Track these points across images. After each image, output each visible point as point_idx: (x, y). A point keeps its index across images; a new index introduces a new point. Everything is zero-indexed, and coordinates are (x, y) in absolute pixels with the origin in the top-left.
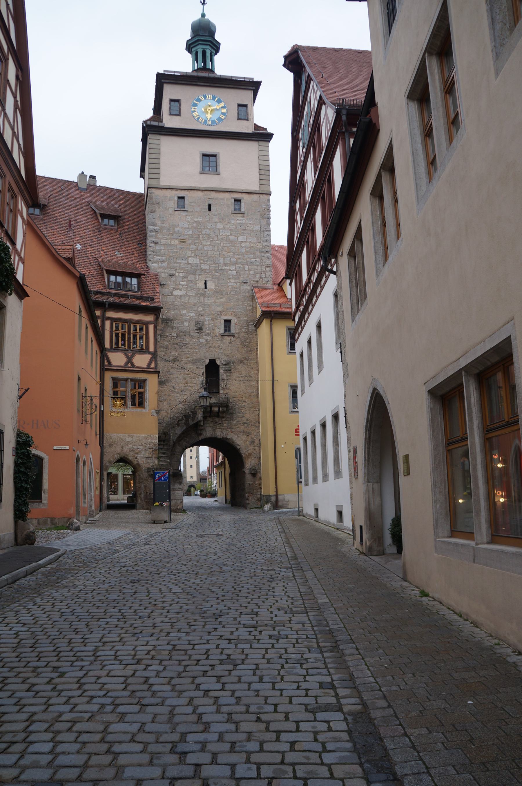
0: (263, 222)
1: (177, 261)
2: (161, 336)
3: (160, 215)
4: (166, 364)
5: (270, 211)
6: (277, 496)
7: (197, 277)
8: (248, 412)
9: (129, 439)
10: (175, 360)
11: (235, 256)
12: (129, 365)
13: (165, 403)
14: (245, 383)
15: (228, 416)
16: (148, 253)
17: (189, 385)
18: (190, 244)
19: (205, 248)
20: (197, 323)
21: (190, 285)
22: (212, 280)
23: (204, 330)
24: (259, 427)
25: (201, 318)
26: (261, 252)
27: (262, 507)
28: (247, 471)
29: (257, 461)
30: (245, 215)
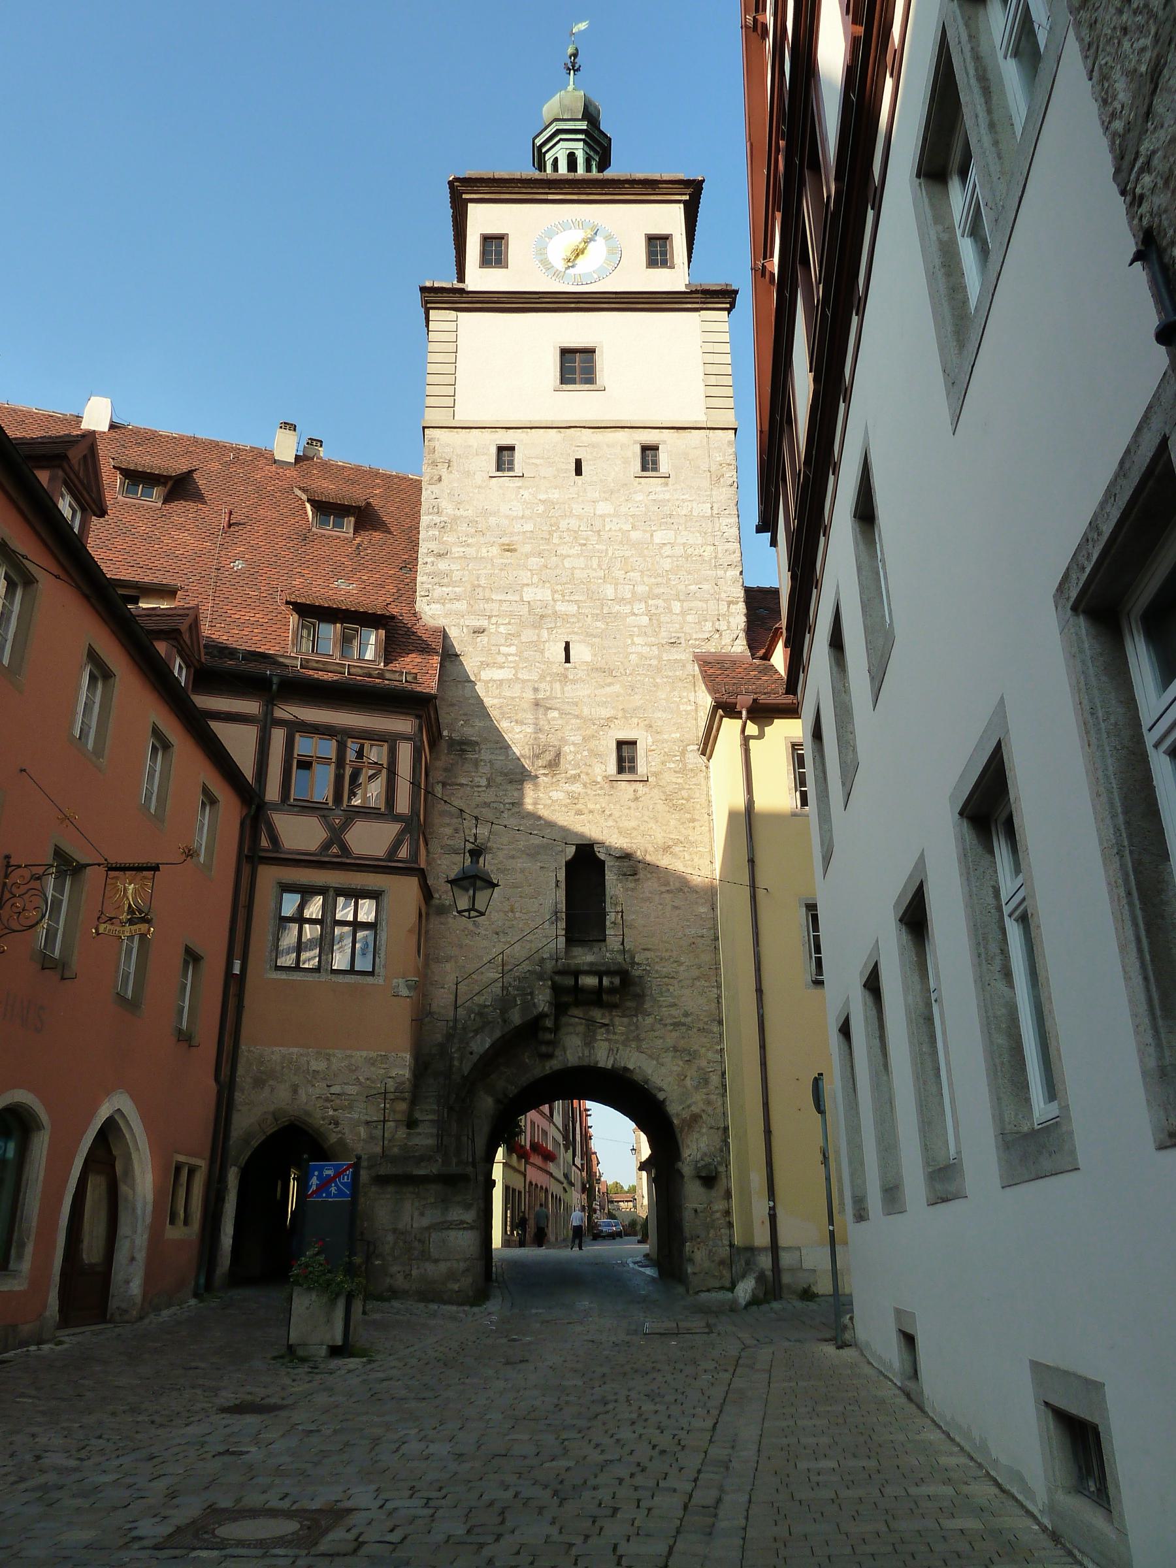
2: (444, 785)
6: (774, 1247)
8: (687, 992)
9: (318, 1065)
11: (645, 579)
12: (335, 850)
14: (677, 908)
15: (629, 1004)
18: (527, 556)
19: (567, 563)
21: (526, 654)
23: (563, 764)
24: (721, 1035)
28: (687, 1170)
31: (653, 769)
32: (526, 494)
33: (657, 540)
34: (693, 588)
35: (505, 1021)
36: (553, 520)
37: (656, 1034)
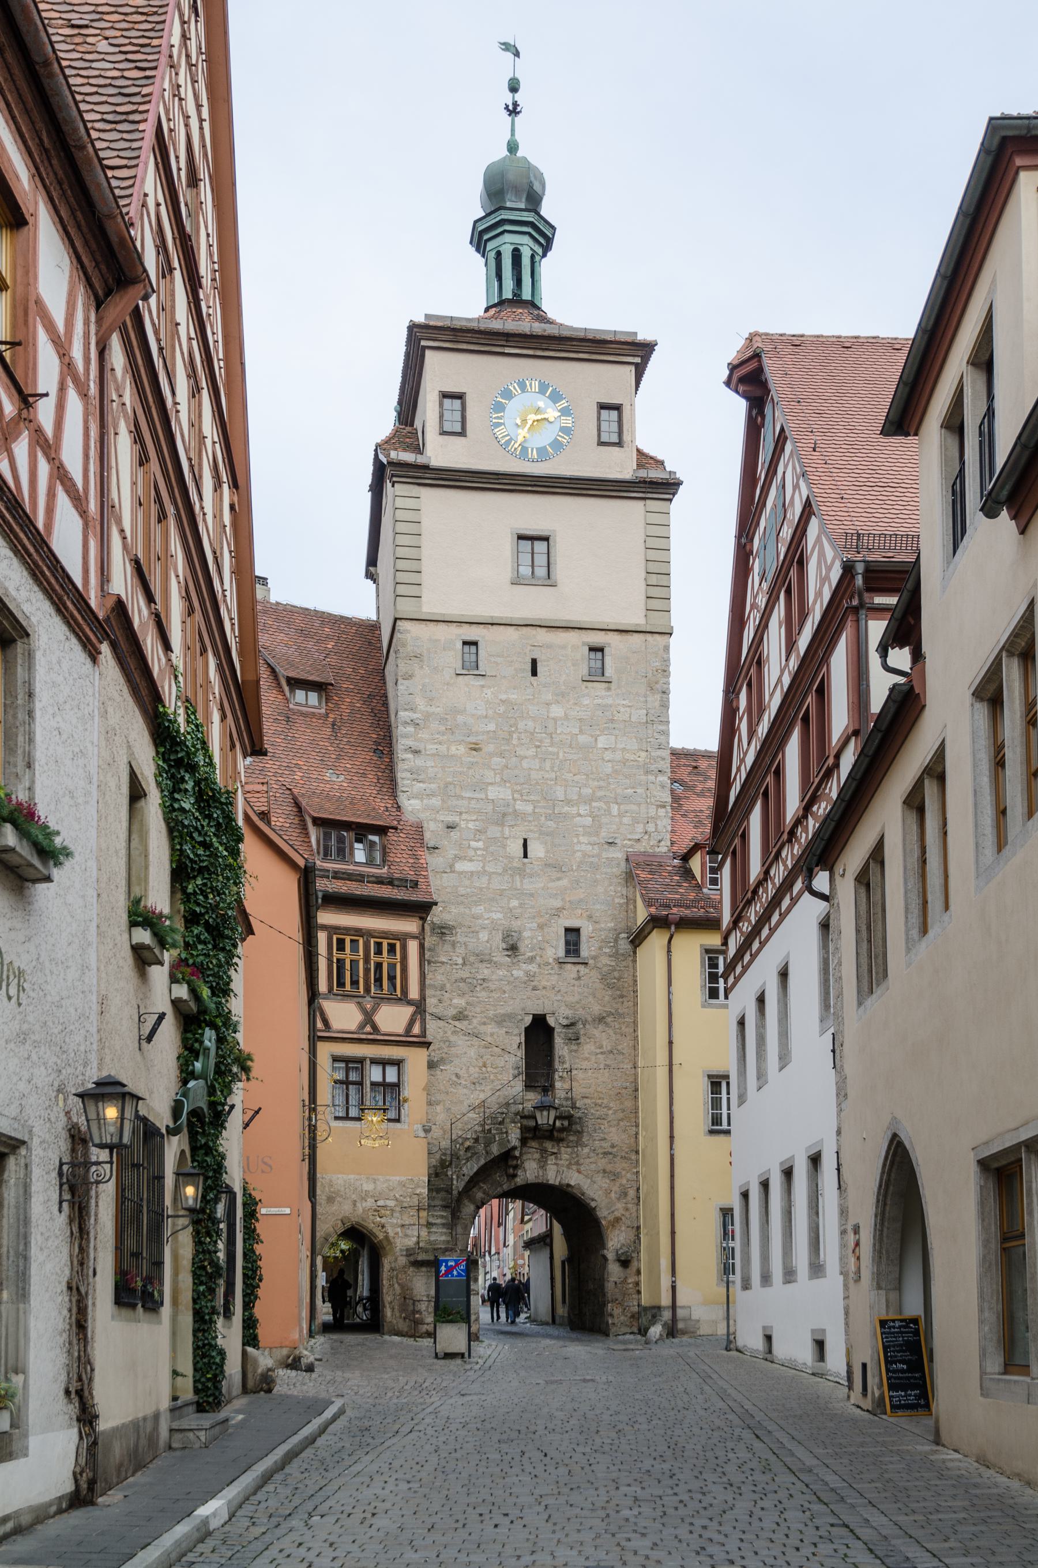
0: (655, 700)
1: (464, 794)
3: (424, 685)
4: (441, 1023)
5: (668, 676)
6: (674, 1306)
7: (507, 830)
8: (613, 1129)
10: (460, 1016)
11: (590, 782)
13: (439, 1108)
14: (607, 1066)
15: (571, 1138)
16: (399, 775)
17: (489, 1069)
18: (491, 755)
19: (525, 764)
20: (507, 936)
22: (539, 838)
23: (522, 947)
24: (637, 1161)
25: (516, 924)
26: (647, 772)
27: (643, 1331)
28: (610, 1256)
29: (632, 1234)
30: (613, 686)
31: (593, 953)
32: (489, 692)
33: (600, 745)
34: (630, 791)
35: (487, 1153)
36: (512, 721)
37: (591, 1160)
